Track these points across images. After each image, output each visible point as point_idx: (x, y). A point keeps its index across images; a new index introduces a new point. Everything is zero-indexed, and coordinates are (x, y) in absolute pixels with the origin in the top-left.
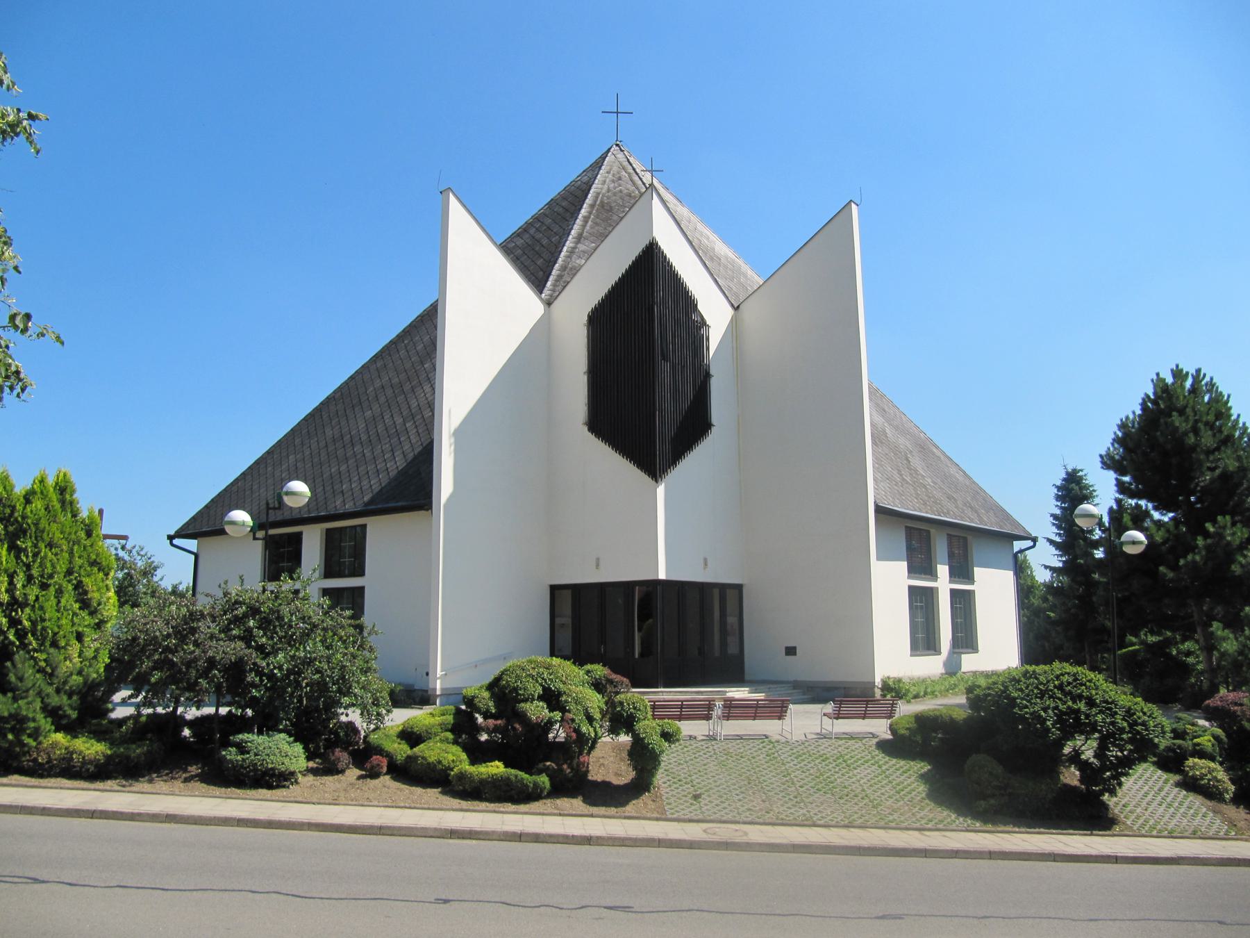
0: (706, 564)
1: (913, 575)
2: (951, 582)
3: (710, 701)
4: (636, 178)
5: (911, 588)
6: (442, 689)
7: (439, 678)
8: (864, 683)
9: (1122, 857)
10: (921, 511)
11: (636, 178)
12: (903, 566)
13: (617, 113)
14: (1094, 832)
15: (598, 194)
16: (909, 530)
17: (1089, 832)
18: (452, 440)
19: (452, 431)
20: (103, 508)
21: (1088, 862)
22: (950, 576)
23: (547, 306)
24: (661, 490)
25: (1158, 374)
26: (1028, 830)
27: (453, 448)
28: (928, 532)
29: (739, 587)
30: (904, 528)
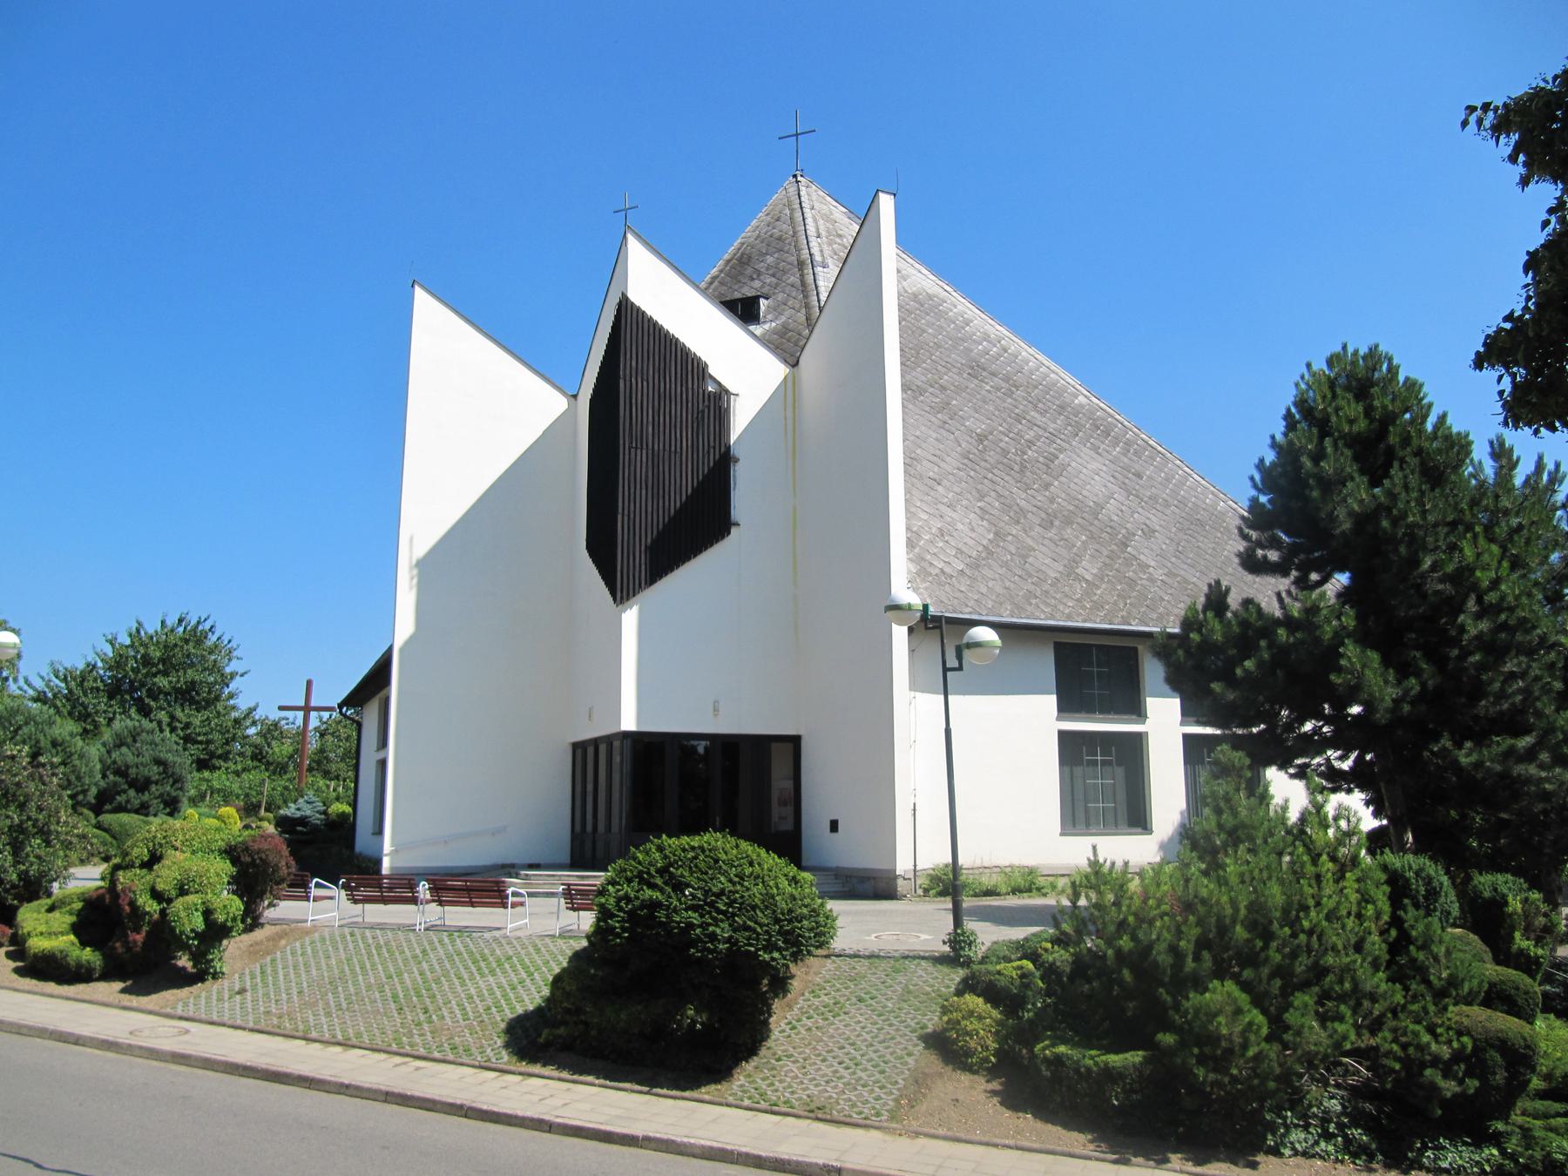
0: (716, 710)
1: (1066, 715)
2: (1183, 723)
3: (410, 880)
4: (798, 214)
5: (1186, 737)
6: (392, 868)
7: (386, 855)
8: (873, 870)
9: (559, 1125)
10: (1053, 617)
11: (798, 214)
12: (1052, 700)
13: (797, 135)
14: (655, 1090)
15: (743, 244)
16: (1059, 648)
17: (646, 1089)
18: (415, 572)
19: (414, 562)
20: (312, 678)
21: (510, 1125)
22: (1183, 715)
23: (573, 399)
24: (630, 618)
25: (1309, 366)
26: (608, 1083)
27: (415, 581)
28: (1135, 649)
29: (795, 741)
30: (1052, 646)
